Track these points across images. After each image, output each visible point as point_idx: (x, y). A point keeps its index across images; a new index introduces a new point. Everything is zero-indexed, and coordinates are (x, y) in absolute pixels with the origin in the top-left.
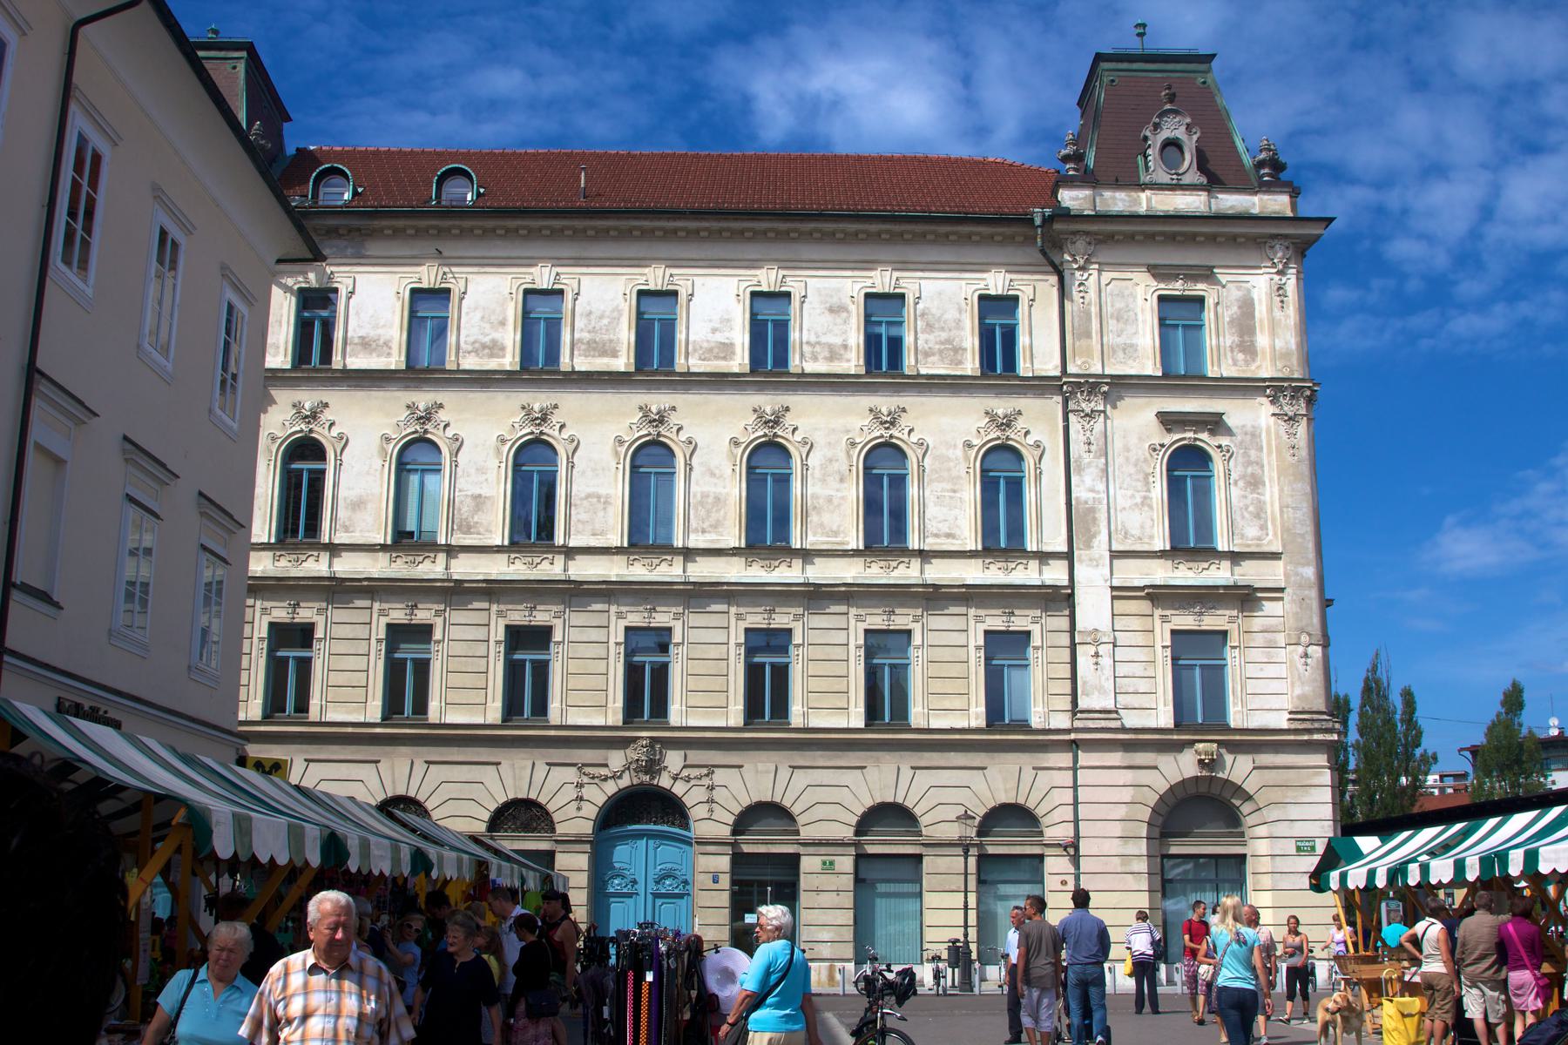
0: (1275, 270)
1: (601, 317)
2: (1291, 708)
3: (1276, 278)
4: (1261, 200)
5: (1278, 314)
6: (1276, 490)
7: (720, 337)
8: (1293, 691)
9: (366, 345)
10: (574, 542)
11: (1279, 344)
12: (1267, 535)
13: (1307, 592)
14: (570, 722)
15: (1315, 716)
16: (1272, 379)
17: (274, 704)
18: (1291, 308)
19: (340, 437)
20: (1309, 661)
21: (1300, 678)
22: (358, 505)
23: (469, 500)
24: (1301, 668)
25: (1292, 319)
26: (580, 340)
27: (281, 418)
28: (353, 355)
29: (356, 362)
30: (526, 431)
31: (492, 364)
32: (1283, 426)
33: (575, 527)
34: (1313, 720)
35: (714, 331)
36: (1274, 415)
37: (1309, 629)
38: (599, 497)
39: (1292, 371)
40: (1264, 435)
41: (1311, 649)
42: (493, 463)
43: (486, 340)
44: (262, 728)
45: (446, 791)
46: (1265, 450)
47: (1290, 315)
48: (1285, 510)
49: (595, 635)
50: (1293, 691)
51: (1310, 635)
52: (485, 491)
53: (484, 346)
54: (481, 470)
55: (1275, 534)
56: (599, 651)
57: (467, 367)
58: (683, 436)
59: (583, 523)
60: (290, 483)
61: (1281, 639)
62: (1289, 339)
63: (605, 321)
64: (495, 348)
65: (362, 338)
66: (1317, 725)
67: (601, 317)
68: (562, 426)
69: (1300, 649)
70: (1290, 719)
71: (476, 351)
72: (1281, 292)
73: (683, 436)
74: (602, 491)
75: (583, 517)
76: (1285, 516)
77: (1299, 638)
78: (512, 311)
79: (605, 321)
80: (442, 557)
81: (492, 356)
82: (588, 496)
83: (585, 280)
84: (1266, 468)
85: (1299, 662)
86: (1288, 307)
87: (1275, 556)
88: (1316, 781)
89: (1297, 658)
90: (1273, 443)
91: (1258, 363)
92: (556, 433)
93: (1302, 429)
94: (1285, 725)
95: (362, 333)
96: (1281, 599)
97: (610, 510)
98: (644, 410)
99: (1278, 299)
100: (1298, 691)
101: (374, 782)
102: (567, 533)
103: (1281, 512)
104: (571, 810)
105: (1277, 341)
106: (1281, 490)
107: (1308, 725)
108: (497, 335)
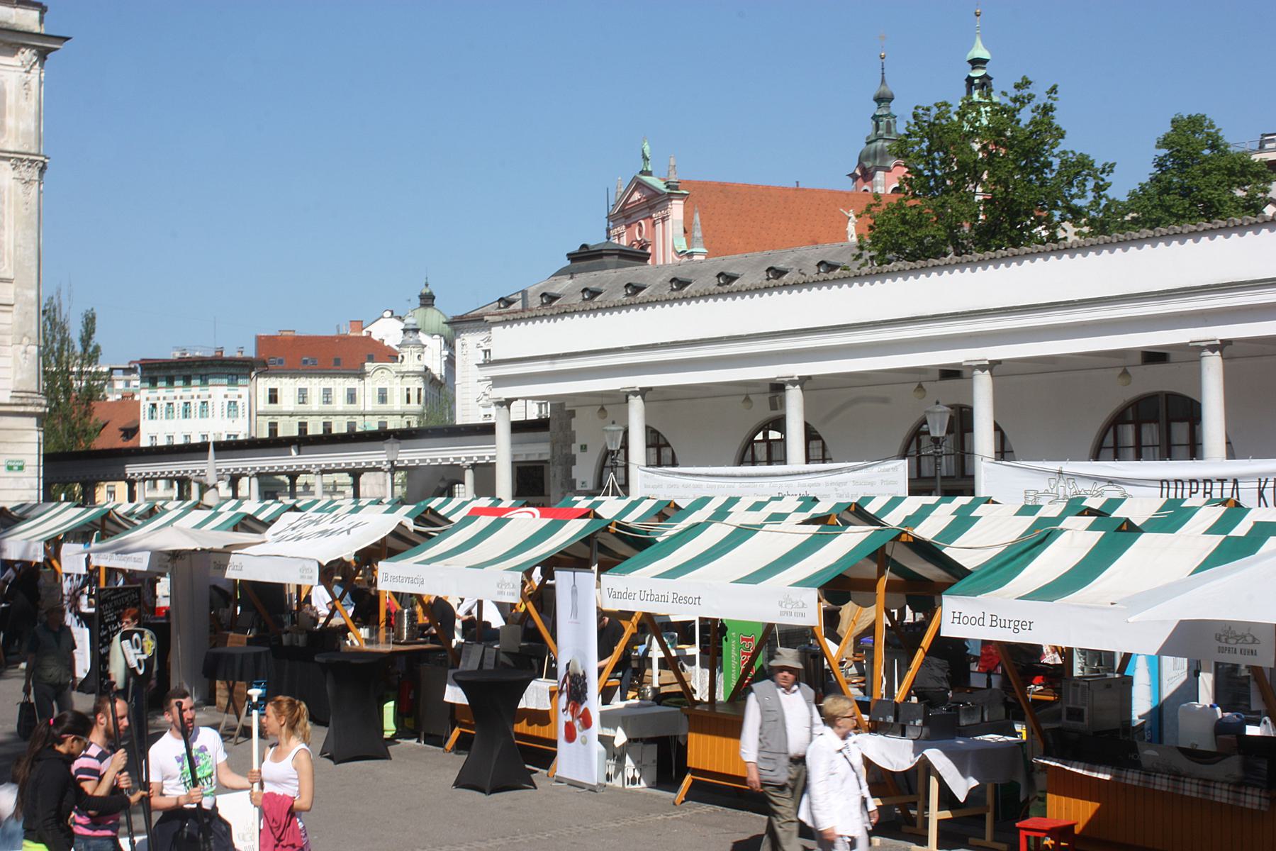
0: (24, 70)
2: (12, 388)
3: (25, 75)
4: (17, 13)
5: (23, 103)
6: (12, 233)
8: (15, 377)
11: (22, 126)
12: (4, 265)
13: (29, 308)
15: (29, 395)
16: (15, 153)
18: (34, 99)
20: (28, 356)
21: (20, 368)
24: (22, 361)
25: (34, 107)
32: (21, 187)
34: (28, 397)
36: (14, 178)
37: (29, 335)
39: (30, 148)
40: (6, 193)
41: (30, 348)
46: (6, 203)
47: (31, 106)
48: (18, 248)
50: (15, 377)
51: (30, 338)
55: (10, 265)
61: (9, 339)
62: (29, 123)
66: (30, 401)
69: (22, 348)
70: (11, 397)
72: (26, 86)
76: (18, 253)
77: (22, 340)
84: (6, 217)
85: (21, 357)
86: (31, 99)
87: (9, 281)
88: (27, 439)
89: (19, 353)
90: (13, 199)
91: (5, 139)
93: (34, 189)
94: (8, 401)
96: (11, 312)
99: (25, 92)
100: (18, 377)
103: (15, 251)
105: (21, 123)
106: (16, 234)
107: (24, 401)
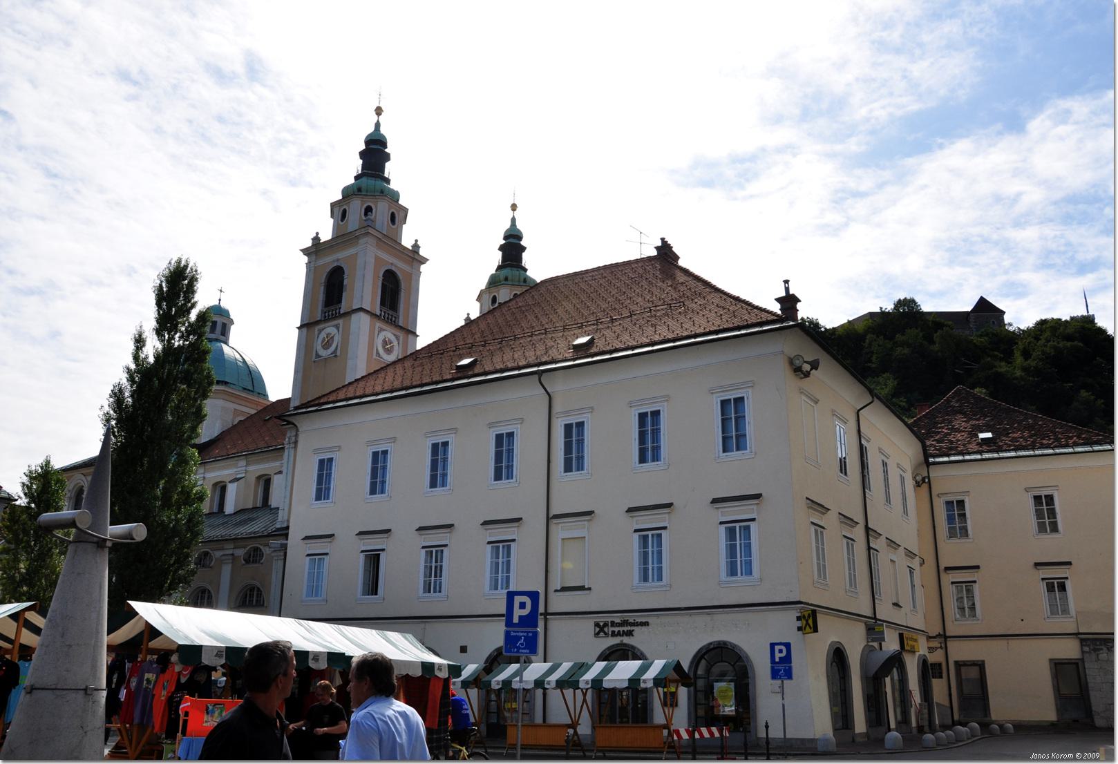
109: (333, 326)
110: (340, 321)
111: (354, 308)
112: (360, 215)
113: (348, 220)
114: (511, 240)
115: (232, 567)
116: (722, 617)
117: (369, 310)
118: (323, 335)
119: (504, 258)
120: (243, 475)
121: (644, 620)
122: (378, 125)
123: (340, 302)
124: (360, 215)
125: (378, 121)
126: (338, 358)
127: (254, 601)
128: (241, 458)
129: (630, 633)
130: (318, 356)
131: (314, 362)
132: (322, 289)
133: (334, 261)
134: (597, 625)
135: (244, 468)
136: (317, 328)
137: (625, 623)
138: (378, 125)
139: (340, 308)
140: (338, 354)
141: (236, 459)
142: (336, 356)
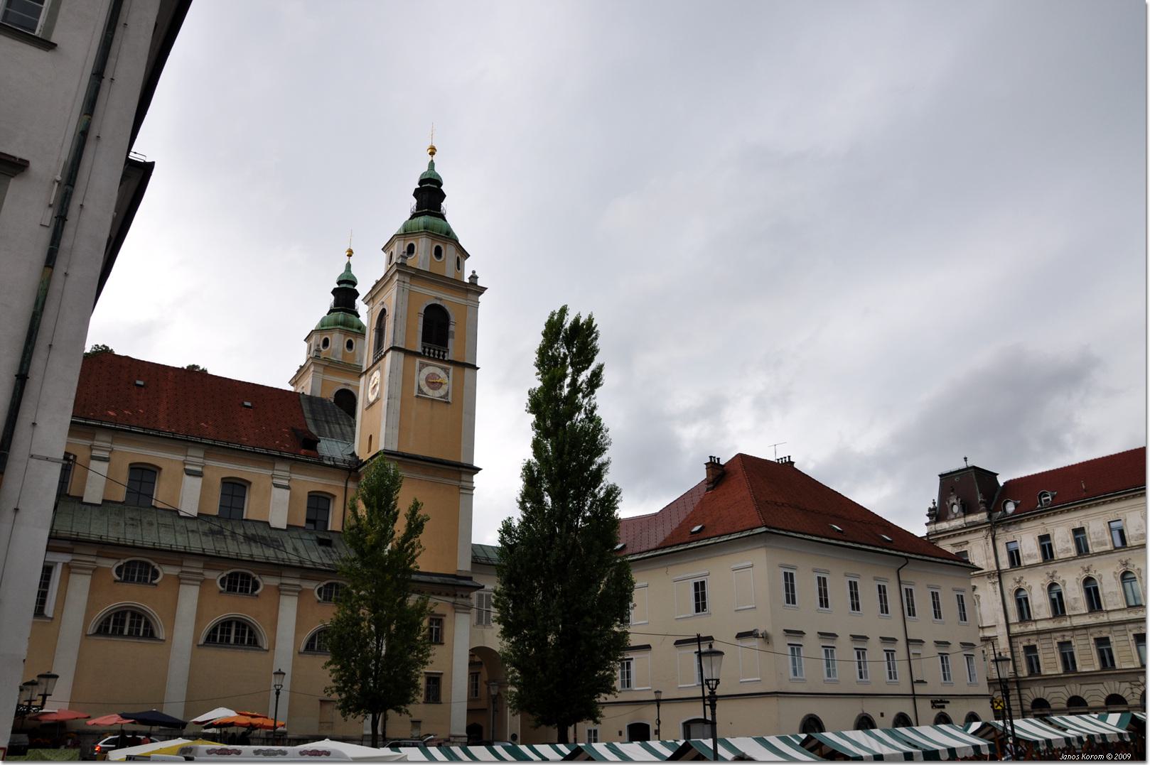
1: (1098, 533)
7: (1139, 532)
9: (1029, 556)
10: (1108, 609)
14: (1123, 667)
17: (1032, 672)
19: (1029, 586)
22: (1040, 606)
23: (1073, 600)
26: (1094, 542)
27: (1010, 584)
28: (1026, 560)
29: (1028, 562)
30: (1084, 576)
31: (1068, 555)
33: (1107, 603)
35: (1137, 530)
38: (1113, 592)
42: (1076, 587)
43: (1064, 548)
44: (1029, 679)
45: (1089, 693)
49: (1123, 638)
52: (1076, 596)
53: (1065, 550)
54: (1074, 590)
56: (1126, 643)
57: (1061, 558)
58: (1136, 568)
59: (1110, 601)
60: (1019, 602)
63: (1100, 534)
64: (1068, 550)
65: (1028, 555)
67: (1098, 533)
68: (1095, 571)
71: (1062, 552)
73: (1136, 568)
74: (1114, 590)
75: (1110, 599)
78: (1070, 536)
79: (1100, 534)
80: (1068, 618)
81: (1068, 552)
82: (1110, 593)
83: (1090, 523)
92: (1093, 574)
95: (1027, 553)
97: (1118, 596)
98: (1121, 561)
101: (1066, 692)
102: (1105, 606)
104: (1131, 696)
108: (1067, 546)
109: (442, 368)
110: (451, 368)
111: (467, 361)
112: (431, 255)
113: (445, 259)
114: (344, 285)
115: (92, 579)
116: (972, 701)
117: (403, 346)
118: (426, 371)
119: (337, 303)
120: (199, 469)
121: (946, 700)
122: (432, 164)
123: (446, 345)
124: (431, 255)
125: (432, 161)
126: (449, 406)
127: (316, 646)
128: (201, 446)
129: (943, 707)
130: (420, 390)
131: (417, 396)
132: (421, 320)
133: (436, 298)
134: (932, 702)
135: (201, 460)
136: (418, 360)
137: (941, 702)
138: (432, 164)
139: (444, 352)
140: (450, 400)
141: (190, 444)
142: (448, 403)
